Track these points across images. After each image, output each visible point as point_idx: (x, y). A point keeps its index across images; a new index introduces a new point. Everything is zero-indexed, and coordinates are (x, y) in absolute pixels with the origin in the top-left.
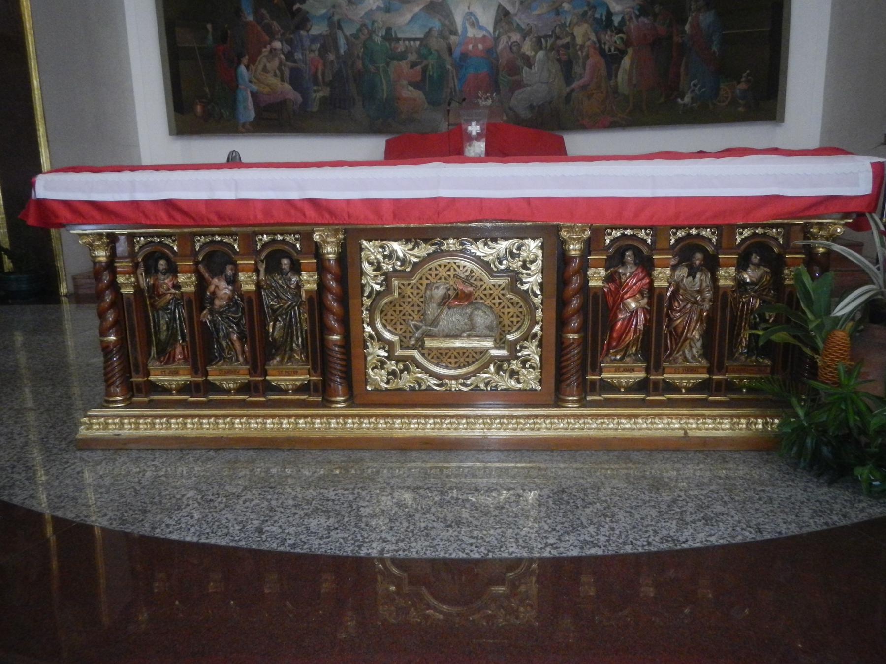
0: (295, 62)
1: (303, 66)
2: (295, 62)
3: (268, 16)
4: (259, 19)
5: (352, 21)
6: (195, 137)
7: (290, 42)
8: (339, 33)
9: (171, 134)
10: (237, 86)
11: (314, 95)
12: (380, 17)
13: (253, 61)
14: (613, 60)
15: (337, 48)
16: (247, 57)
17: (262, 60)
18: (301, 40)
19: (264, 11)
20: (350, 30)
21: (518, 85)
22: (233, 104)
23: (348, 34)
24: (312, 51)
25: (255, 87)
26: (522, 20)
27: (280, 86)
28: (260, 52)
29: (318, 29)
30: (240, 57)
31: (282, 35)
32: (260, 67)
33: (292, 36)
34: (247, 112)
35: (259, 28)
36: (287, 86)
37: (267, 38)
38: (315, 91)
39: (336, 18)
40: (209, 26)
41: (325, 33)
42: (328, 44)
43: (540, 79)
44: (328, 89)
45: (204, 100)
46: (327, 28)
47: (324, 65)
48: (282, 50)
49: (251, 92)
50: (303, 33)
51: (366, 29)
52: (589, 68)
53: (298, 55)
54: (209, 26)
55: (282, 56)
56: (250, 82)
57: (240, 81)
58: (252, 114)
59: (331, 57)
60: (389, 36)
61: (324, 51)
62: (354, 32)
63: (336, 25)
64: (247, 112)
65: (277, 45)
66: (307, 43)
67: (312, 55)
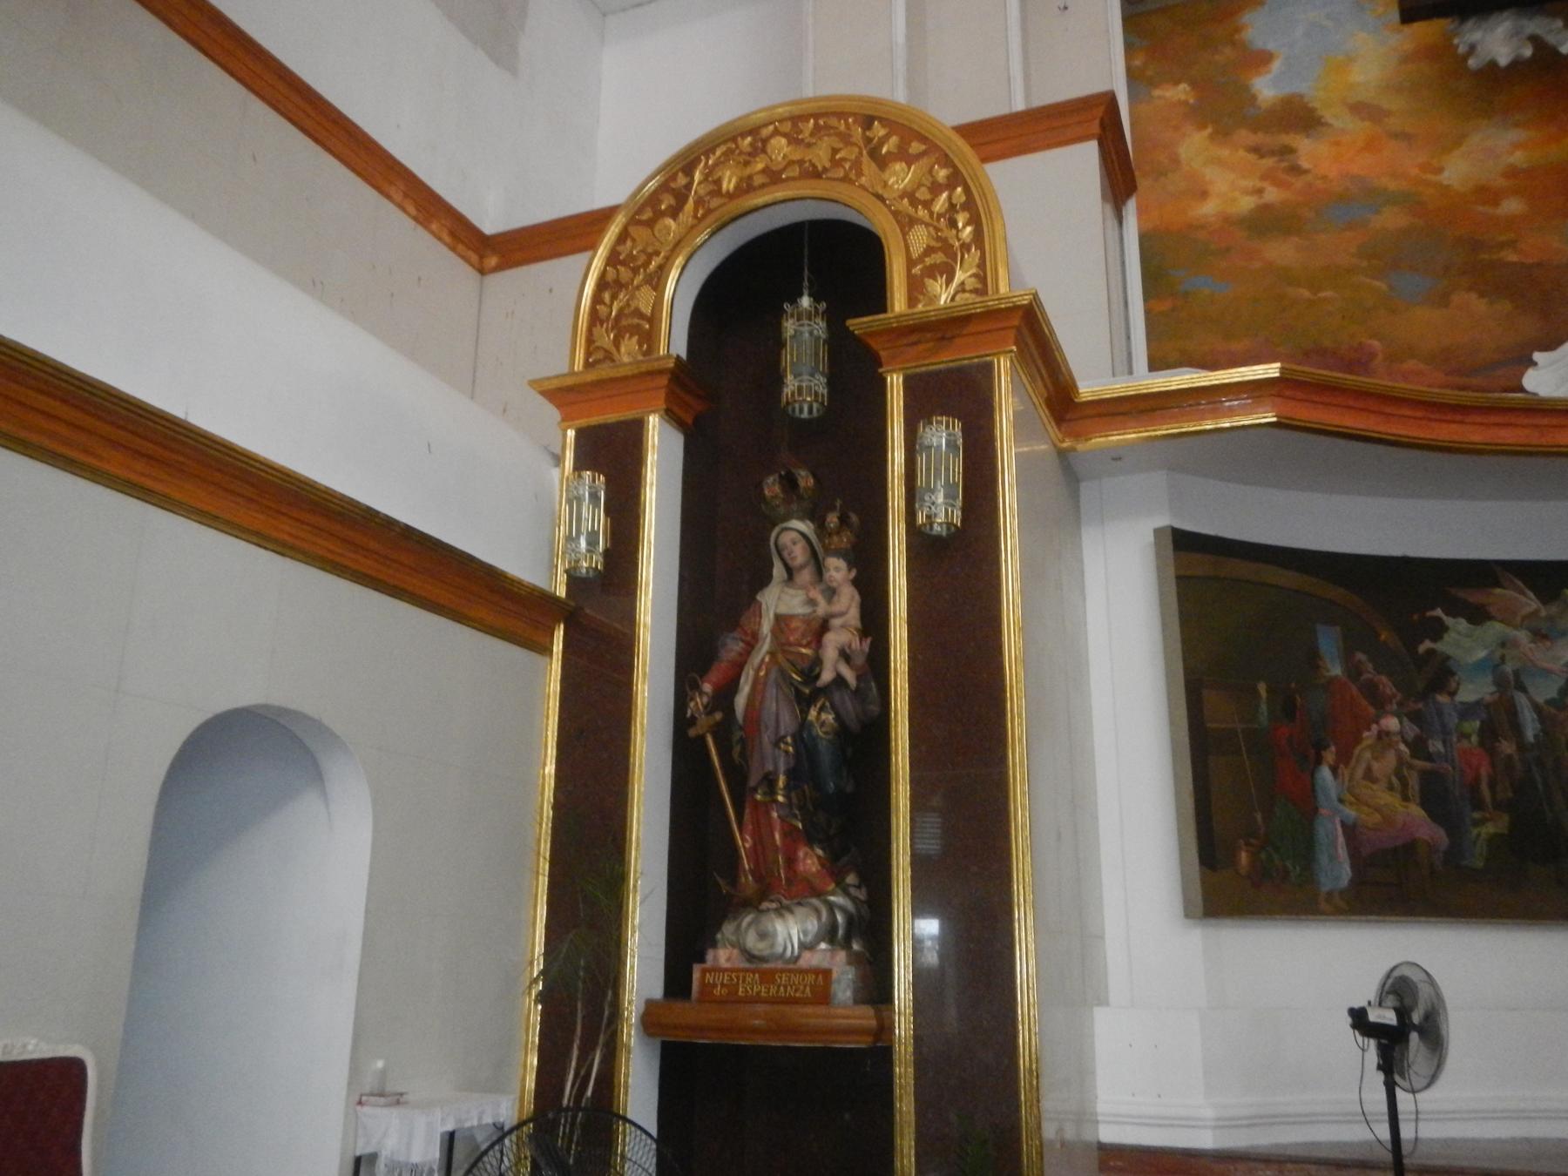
0: (1429, 757)
1: (1445, 765)
2: (1429, 757)
3: (1370, 666)
4: (1354, 672)
5: (1547, 673)
6: (1228, 922)
7: (1416, 717)
8: (1521, 700)
9: (1188, 914)
10: (1316, 810)
11: (1475, 831)
13: (1345, 757)
15: (1517, 728)
16: (1333, 748)
17: (1364, 753)
18: (1440, 714)
19: (1360, 656)
20: (1544, 691)
22: (1306, 850)
23: (1540, 700)
24: (1464, 736)
25: (1350, 813)
27: (1401, 809)
28: (1358, 740)
29: (1474, 690)
30: (1320, 747)
31: (1400, 704)
32: (1360, 772)
33: (1420, 705)
35: (1354, 689)
36: (1416, 811)
37: (1372, 710)
38: (1476, 823)
39: (1508, 668)
40: (1262, 688)
41: (1488, 698)
42: (1497, 720)
44: (1506, 818)
45: (1253, 841)
46: (1493, 689)
47: (1493, 765)
48: (1401, 733)
49: (1343, 824)
50: (1442, 699)
53: (1436, 746)
54: (1262, 688)
55: (1402, 747)
56: (1341, 801)
57: (1321, 798)
58: (1345, 873)
59: (1507, 747)
61: (1489, 734)
62: (1552, 693)
64: (1337, 869)
65: (1392, 723)
66: (1452, 720)
67: (1465, 743)
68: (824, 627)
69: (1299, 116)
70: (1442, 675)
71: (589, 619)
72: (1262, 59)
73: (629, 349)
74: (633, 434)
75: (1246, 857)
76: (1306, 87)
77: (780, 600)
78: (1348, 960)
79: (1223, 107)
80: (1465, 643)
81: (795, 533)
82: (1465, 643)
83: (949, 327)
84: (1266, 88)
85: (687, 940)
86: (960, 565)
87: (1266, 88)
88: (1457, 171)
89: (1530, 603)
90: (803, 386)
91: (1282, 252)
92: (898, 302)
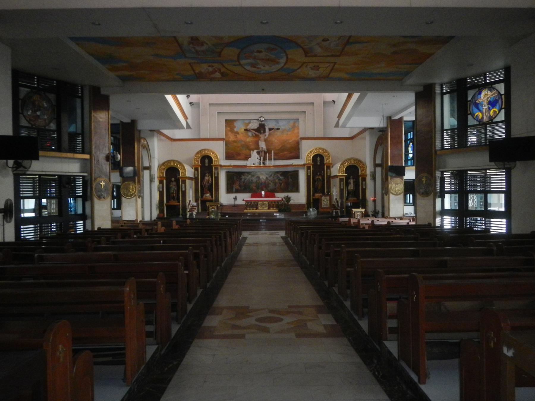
12: (251, 179)
14: (281, 184)
26: (269, 178)
29: (243, 180)
34: (234, 190)
42: (244, 182)
52: (278, 185)
63: (245, 179)
64: (234, 190)
68: (209, 180)
69: (237, 133)
70: (241, 179)
71: (196, 179)
72: (235, 127)
73: (197, 163)
75: (229, 190)
76: (239, 131)
77: (206, 178)
78: (233, 195)
79: (232, 130)
80: (243, 177)
81: (207, 174)
82: (243, 177)
84: (235, 130)
85: (202, 196)
86: (217, 179)
87: (235, 130)
88: (248, 140)
89: (247, 174)
90: (207, 165)
91: (235, 144)
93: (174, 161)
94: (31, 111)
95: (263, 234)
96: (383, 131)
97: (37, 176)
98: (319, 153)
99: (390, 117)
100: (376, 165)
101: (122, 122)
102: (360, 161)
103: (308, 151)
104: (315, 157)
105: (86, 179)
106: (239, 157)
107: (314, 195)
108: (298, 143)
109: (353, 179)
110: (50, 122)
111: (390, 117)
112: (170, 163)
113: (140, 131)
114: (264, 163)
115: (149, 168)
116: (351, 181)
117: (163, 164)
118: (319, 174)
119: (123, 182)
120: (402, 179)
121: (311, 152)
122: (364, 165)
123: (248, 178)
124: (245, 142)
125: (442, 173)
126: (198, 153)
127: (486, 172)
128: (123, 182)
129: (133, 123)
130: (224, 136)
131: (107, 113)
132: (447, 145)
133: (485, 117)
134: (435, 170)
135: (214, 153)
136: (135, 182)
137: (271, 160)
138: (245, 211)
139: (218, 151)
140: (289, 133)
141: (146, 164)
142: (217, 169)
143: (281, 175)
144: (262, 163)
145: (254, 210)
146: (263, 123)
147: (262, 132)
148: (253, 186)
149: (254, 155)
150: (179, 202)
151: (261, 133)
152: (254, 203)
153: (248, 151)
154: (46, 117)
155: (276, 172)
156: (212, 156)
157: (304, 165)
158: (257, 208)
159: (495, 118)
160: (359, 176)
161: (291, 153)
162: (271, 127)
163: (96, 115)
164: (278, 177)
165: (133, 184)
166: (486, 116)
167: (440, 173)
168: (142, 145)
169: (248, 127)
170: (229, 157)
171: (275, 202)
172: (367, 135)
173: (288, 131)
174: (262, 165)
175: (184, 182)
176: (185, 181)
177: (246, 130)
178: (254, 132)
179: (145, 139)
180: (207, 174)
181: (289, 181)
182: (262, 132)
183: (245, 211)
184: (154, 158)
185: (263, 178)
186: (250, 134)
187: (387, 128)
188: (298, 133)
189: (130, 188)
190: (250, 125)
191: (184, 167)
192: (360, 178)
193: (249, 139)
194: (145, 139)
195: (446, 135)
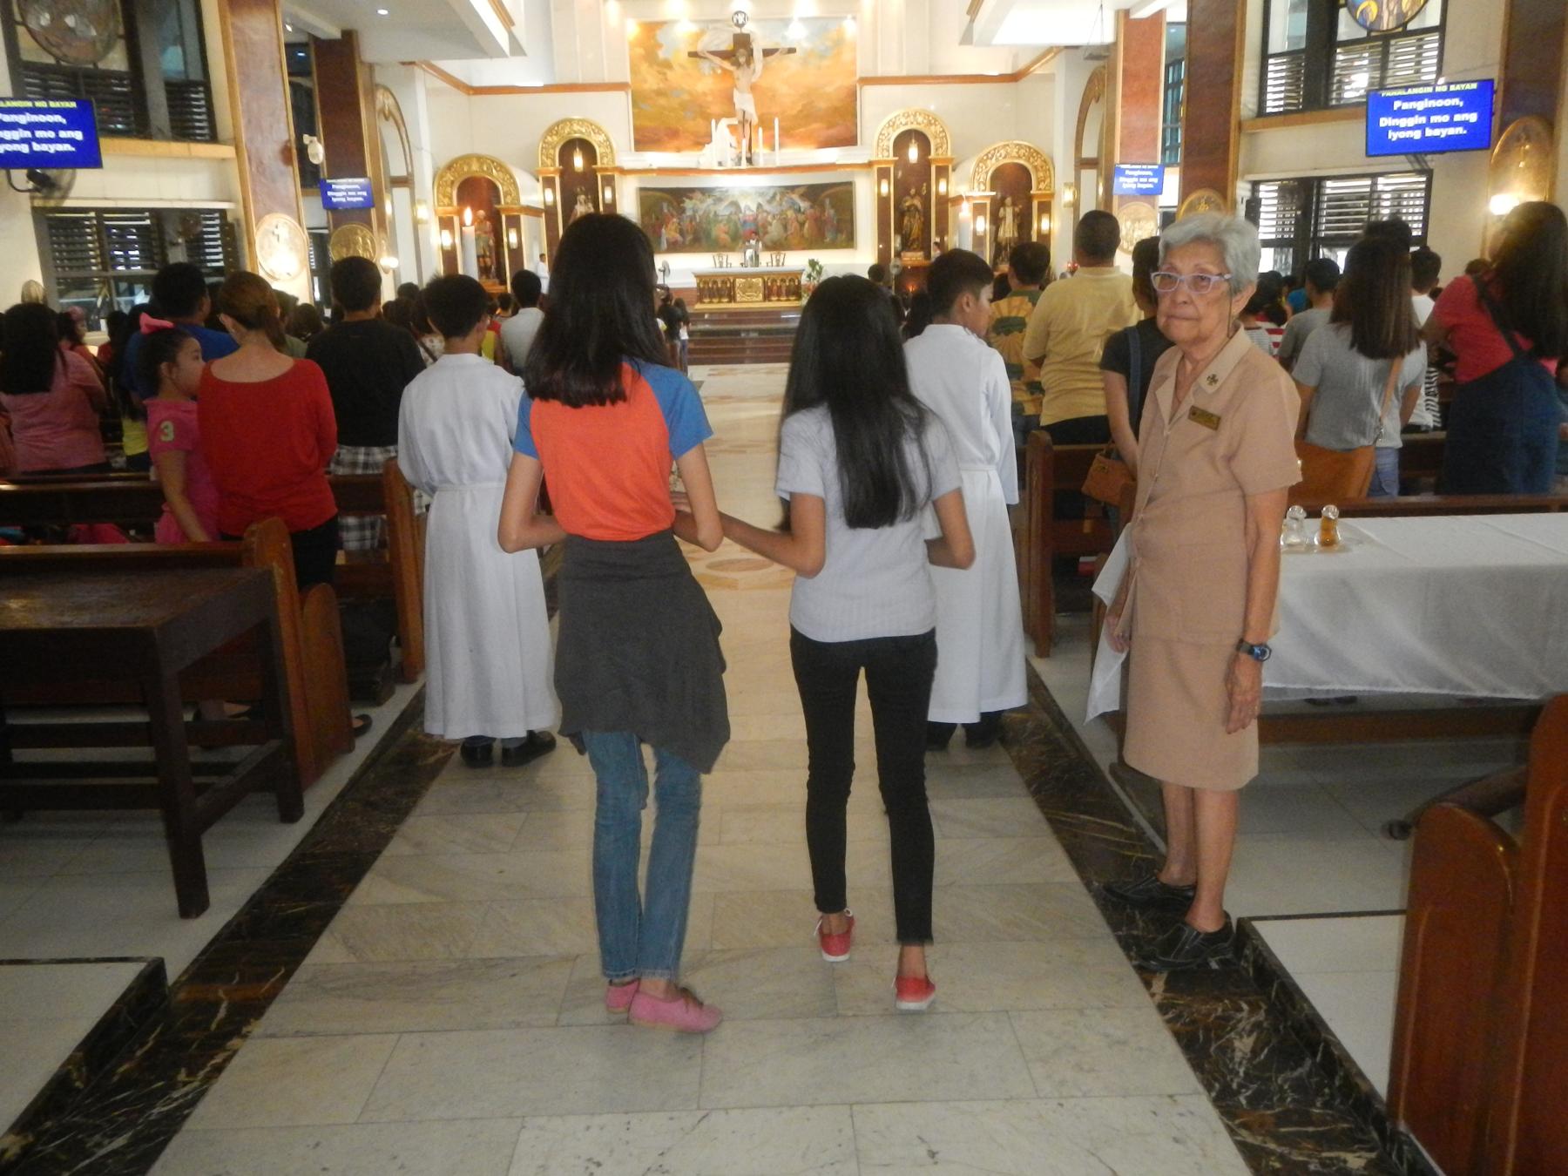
12: (713, 209)
14: (802, 225)
21: (766, 233)
26: (767, 207)
29: (689, 213)
34: (664, 245)
42: (693, 218)
43: (775, 230)
51: (707, 213)
60: (716, 214)
63: (695, 211)
64: (664, 245)
69: (667, 65)
70: (683, 211)
71: (549, 212)
72: (660, 46)
74: (553, 179)
80: (688, 204)
81: (582, 198)
82: (688, 204)
83: (606, 169)
84: (661, 54)
87: (661, 54)
89: (698, 195)
91: (662, 101)
92: (599, 165)
93: (480, 158)
94: (47, 16)
95: (746, 372)
96: (1100, 55)
97: (92, 214)
98: (914, 126)
99: (1127, 12)
100: (1083, 163)
101: (316, 39)
102: (1033, 153)
103: (881, 118)
104: (902, 141)
105: (230, 219)
106: (676, 143)
107: (898, 255)
108: (852, 96)
109: (1014, 204)
110: (108, 47)
111: (1127, 12)
112: (469, 165)
113: (371, 67)
114: (749, 160)
115: (405, 181)
116: (1008, 213)
117: (449, 167)
118: (913, 191)
119: (336, 226)
120: (1153, 206)
121: (891, 124)
122: (1047, 165)
123: (704, 206)
124: (690, 93)
125: (1255, 185)
126: (550, 131)
127: (1374, 184)
128: (336, 226)
129: (349, 39)
130: (628, 78)
131: (272, 16)
132: (1273, 103)
133: (1385, 15)
134: (1235, 178)
135: (599, 131)
136: (369, 224)
137: (773, 149)
138: (698, 306)
139: (611, 123)
140: (826, 63)
141: (398, 170)
142: (609, 181)
143: (804, 196)
144: (744, 161)
145: (725, 305)
146: (745, 30)
147: (742, 60)
148: (719, 231)
149: (721, 132)
150: (504, 282)
151: (738, 65)
152: (724, 282)
153: (700, 121)
154: (94, 33)
155: (787, 188)
156: (595, 140)
157: (870, 164)
158: (732, 298)
159: (1412, 18)
160: (1030, 199)
161: (828, 128)
162: (770, 46)
163: (240, 24)
164: (794, 203)
165: (366, 231)
166: (1390, 13)
167: (1249, 186)
168: (382, 111)
169: (699, 48)
170: (644, 140)
171: (783, 281)
172: (1056, 66)
173: (822, 57)
174: (744, 165)
175: (514, 222)
176: (518, 218)
177: (693, 55)
178: (717, 60)
179: (387, 89)
180: (582, 198)
181: (826, 212)
182: (742, 60)
183: (698, 306)
184: (420, 149)
185: (749, 206)
186: (705, 67)
187: (1115, 44)
188: (854, 62)
189: (356, 243)
190: (706, 38)
191: (512, 177)
192: (1035, 204)
193: (704, 82)
194: (387, 89)
195: (1277, 70)
